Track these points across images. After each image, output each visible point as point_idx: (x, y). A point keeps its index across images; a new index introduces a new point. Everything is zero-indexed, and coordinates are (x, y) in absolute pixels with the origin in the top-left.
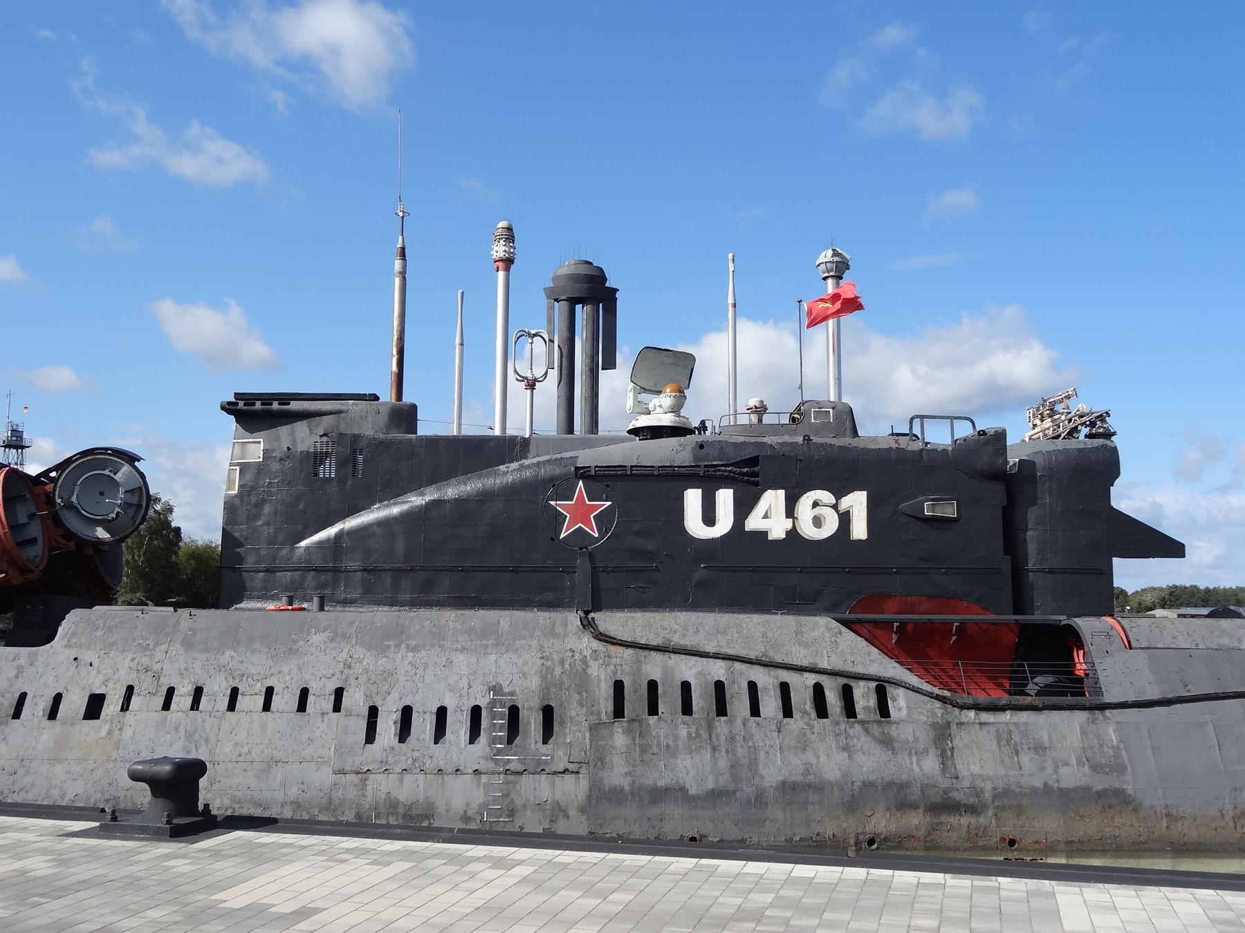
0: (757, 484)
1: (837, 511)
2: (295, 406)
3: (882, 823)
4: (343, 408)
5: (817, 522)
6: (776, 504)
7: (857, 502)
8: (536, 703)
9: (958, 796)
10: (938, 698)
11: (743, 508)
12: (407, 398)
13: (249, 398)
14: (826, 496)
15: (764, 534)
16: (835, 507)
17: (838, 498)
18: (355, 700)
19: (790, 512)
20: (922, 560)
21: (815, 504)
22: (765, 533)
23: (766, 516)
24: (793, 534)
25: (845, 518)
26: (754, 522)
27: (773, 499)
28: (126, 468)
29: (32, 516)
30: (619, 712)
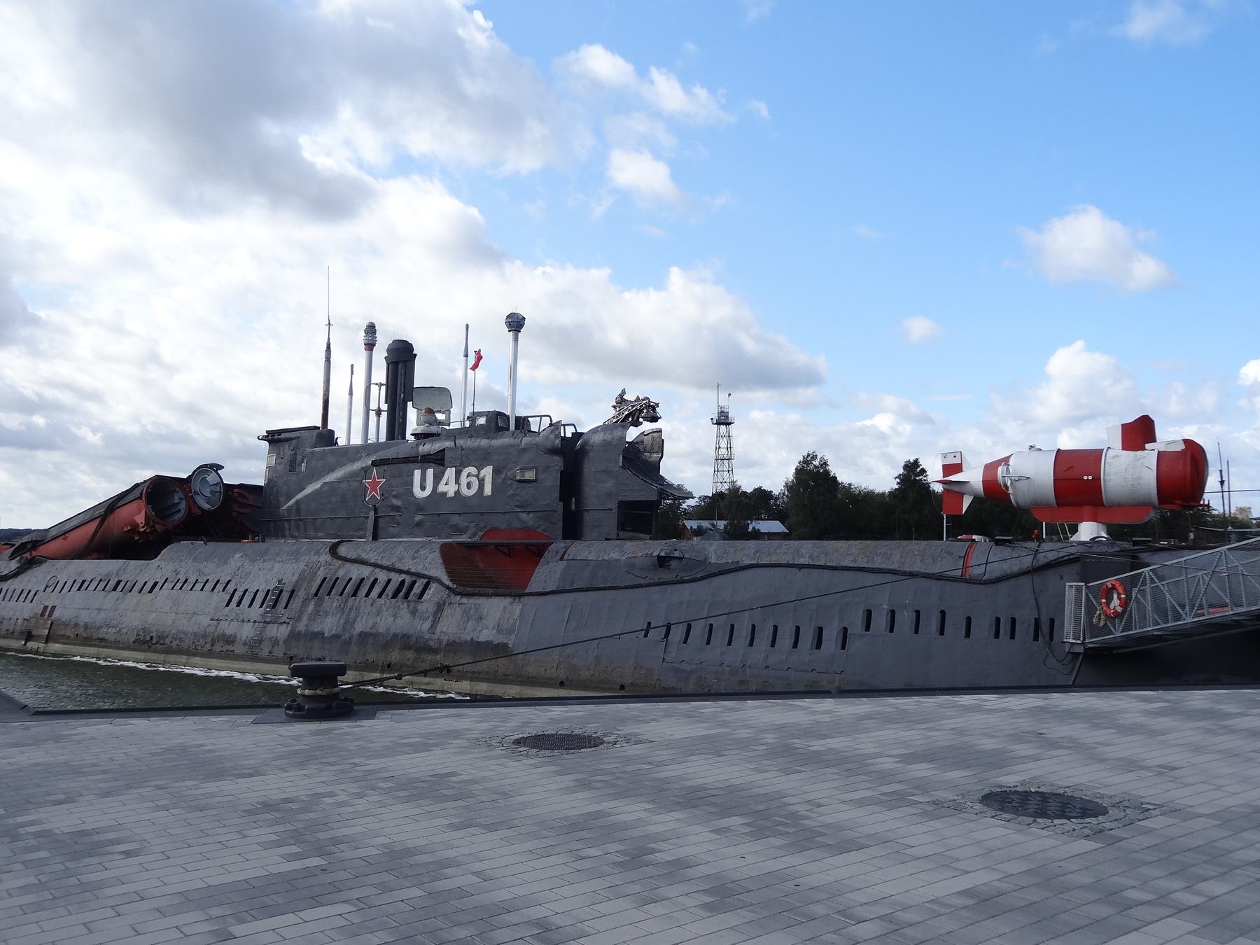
2: (283, 436)
3: (395, 656)
5: (469, 486)
7: (487, 472)
8: (290, 589)
9: (431, 643)
10: (448, 588)
11: (438, 478)
12: (329, 427)
14: (472, 470)
15: (445, 494)
16: (477, 476)
18: (231, 588)
19: (457, 481)
21: (469, 475)
24: (457, 493)
25: (481, 482)
26: (442, 488)
27: (450, 473)
30: (316, 595)
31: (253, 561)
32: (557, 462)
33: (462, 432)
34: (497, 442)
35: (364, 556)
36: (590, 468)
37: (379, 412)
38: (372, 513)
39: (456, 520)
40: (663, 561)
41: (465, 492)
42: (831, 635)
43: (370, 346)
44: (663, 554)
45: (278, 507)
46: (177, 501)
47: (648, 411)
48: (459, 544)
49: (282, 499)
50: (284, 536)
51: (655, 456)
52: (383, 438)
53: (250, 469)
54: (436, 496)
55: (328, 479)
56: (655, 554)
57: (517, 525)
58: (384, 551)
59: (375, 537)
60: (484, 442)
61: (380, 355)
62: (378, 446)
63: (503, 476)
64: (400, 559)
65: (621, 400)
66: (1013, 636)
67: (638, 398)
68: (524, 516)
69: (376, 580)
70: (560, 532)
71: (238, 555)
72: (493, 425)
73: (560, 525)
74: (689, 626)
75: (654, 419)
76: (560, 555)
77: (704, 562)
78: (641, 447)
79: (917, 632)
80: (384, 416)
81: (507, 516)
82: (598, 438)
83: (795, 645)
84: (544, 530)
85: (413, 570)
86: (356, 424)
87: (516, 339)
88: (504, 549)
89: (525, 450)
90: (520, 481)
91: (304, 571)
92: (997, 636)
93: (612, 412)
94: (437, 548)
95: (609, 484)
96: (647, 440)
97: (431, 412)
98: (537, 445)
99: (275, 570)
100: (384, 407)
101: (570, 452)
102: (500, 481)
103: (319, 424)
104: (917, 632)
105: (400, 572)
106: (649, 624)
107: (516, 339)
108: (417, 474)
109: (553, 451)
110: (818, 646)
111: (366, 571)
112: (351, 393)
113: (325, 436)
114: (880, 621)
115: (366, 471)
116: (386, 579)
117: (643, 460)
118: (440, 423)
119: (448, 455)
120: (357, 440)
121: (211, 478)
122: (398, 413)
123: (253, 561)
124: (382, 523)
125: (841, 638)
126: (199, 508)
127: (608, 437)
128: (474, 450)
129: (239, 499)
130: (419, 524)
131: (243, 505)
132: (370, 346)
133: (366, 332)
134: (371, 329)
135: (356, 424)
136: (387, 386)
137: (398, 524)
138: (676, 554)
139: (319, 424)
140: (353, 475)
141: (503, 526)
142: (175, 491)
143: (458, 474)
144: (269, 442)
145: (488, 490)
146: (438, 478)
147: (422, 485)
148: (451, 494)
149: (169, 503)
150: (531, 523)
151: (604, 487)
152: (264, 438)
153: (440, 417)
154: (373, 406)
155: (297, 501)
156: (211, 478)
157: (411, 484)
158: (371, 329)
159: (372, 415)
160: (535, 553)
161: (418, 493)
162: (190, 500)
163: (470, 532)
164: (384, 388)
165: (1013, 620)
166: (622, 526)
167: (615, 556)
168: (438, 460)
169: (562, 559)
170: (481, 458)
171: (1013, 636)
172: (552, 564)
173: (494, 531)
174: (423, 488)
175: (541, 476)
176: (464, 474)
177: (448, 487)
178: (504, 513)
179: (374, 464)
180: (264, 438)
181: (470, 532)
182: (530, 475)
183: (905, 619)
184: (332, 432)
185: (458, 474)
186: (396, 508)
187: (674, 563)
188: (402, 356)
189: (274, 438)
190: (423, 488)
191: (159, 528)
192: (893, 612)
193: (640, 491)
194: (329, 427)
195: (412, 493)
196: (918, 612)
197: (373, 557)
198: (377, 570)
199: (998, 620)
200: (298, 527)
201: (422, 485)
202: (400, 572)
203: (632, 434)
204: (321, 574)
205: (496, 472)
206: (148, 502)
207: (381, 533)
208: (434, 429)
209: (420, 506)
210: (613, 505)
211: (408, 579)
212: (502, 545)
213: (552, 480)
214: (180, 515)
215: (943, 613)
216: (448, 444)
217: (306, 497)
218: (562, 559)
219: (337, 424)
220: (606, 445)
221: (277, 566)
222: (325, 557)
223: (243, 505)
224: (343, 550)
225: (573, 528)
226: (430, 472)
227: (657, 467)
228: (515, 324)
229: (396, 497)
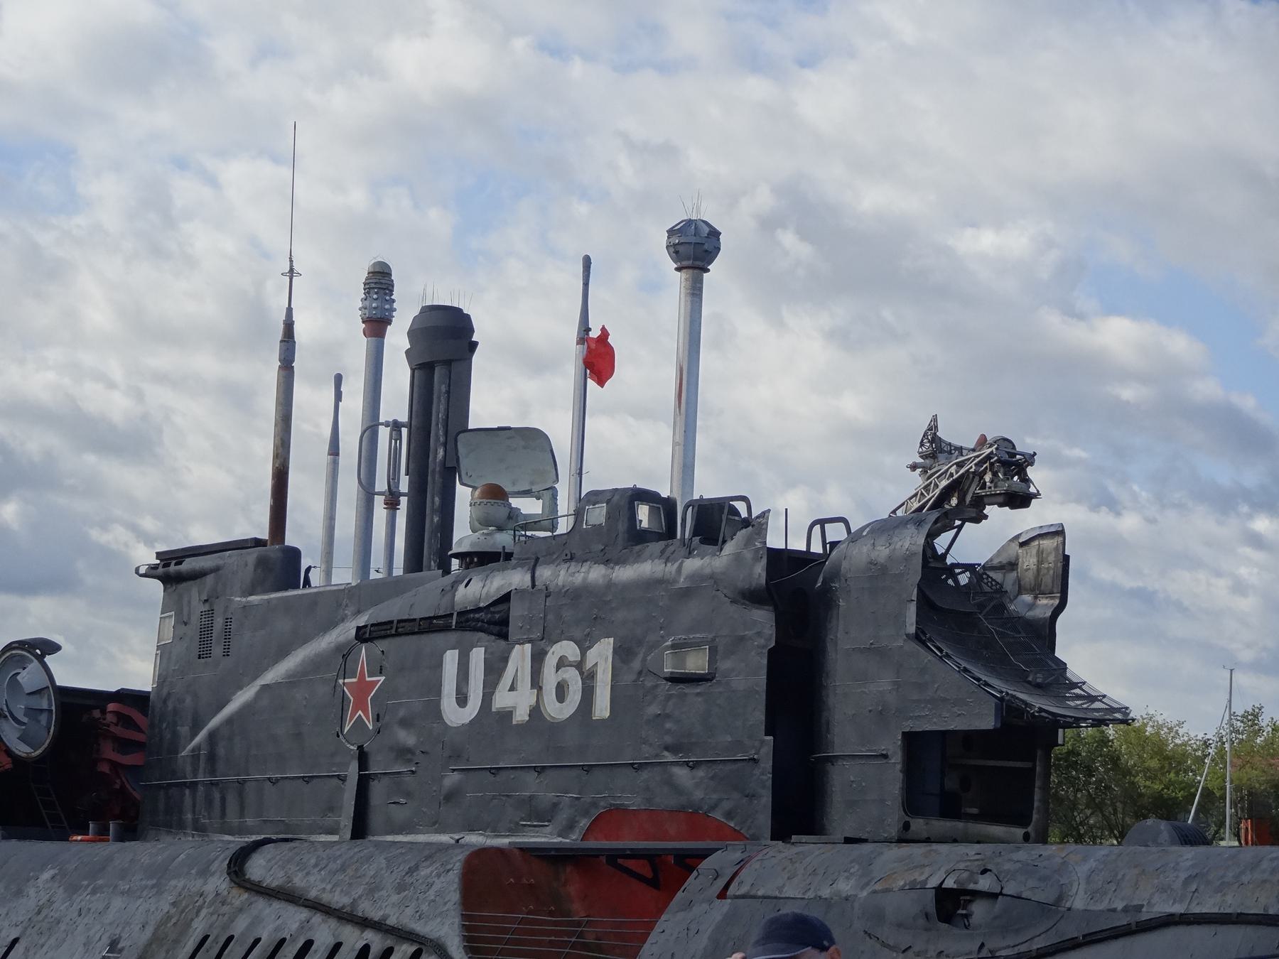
0: (504, 636)
1: (581, 673)
2: (189, 565)
4: (221, 562)
6: (523, 667)
7: (602, 653)
12: (291, 540)
13: (166, 558)
15: (507, 715)
16: (579, 666)
17: (583, 654)
19: (536, 683)
20: (667, 748)
21: (562, 663)
23: (512, 688)
24: (536, 711)
25: (589, 679)
26: (502, 699)
27: (520, 656)
28: (34, 665)
31: (73, 889)
32: (763, 621)
33: (569, 549)
34: (625, 573)
35: (299, 881)
36: (847, 638)
37: (392, 504)
38: (353, 770)
39: (532, 786)
40: (950, 905)
41: (558, 711)
43: (377, 325)
44: (949, 884)
45: (174, 749)
47: (1001, 475)
48: (525, 850)
49: (184, 730)
50: (181, 826)
51: (1045, 605)
52: (398, 570)
53: (116, 650)
54: (493, 722)
55: (270, 677)
56: (933, 883)
57: (665, 800)
58: (343, 869)
59: (360, 830)
60: (595, 574)
61: (397, 339)
62: (390, 587)
63: (636, 665)
64: (373, 890)
65: (935, 447)
67: (983, 441)
68: (681, 774)
69: (309, 944)
70: (764, 820)
71: (46, 875)
72: (622, 526)
73: (766, 799)
75: (1019, 500)
76: (720, 884)
77: (1052, 909)
78: (1009, 581)
80: (404, 501)
81: (645, 775)
82: (862, 553)
84: (729, 815)
85: (392, 921)
86: (344, 534)
87: (695, 291)
88: (644, 869)
89: (686, 594)
90: (675, 679)
91: (168, 917)
93: (916, 481)
94: (457, 862)
95: (883, 684)
96: (1028, 561)
97: (496, 493)
98: (714, 579)
99: (110, 917)
100: (404, 485)
101: (797, 591)
102: (628, 678)
103: (262, 531)
105: (365, 923)
108: (451, 659)
109: (753, 597)
111: (291, 920)
112: (334, 450)
113: (277, 563)
115: (345, 654)
116: (331, 941)
117: (996, 622)
118: (534, 523)
119: (517, 611)
120: (344, 576)
121: (29, 677)
122: (433, 500)
123: (73, 889)
124: (378, 791)
126: (8, 752)
127: (882, 552)
128: (575, 595)
129: (118, 731)
130: (451, 797)
131: (125, 745)
132: (377, 325)
133: (368, 288)
134: (380, 281)
135: (344, 534)
136: (409, 425)
137: (408, 795)
138: (984, 884)
139: (264, 534)
140: (316, 665)
141: (633, 802)
143: (538, 659)
144: (167, 580)
145: (602, 708)
146: (494, 670)
147: (465, 690)
148: (521, 715)
150: (698, 794)
151: (883, 690)
152: (152, 572)
153: (529, 507)
154: (381, 484)
155: (212, 736)
156: (29, 677)
157: (437, 689)
158: (380, 281)
159: (379, 502)
160: (665, 873)
161: (456, 716)
163: (562, 817)
164: (405, 431)
166: (913, 803)
167: (845, 887)
168: (493, 622)
169: (722, 895)
170: (585, 614)
172: (697, 909)
173: (611, 818)
174: (462, 700)
175: (724, 665)
176: (551, 660)
177: (516, 700)
178: (638, 767)
179: (363, 635)
180: (152, 572)
181: (562, 817)
182: (696, 663)
184: (294, 554)
185: (538, 659)
186: (403, 753)
187: (979, 910)
188: (446, 344)
189: (174, 570)
190: (462, 700)
193: (964, 701)
195: (435, 711)
197: (314, 885)
198: (318, 918)
200: (209, 802)
201: (465, 690)
202: (365, 923)
203: (978, 542)
204: (198, 927)
205: (623, 654)
207: (376, 819)
208: (503, 540)
209: (455, 748)
210: (892, 745)
212: (635, 855)
213: (749, 675)
216: (516, 579)
217: (229, 721)
218: (722, 895)
219: (303, 532)
220: (878, 573)
221: (118, 903)
222: (219, 882)
223: (125, 745)
224: (257, 868)
225: (799, 807)
226: (478, 656)
227: (1045, 633)
228: (695, 249)
229: (405, 723)
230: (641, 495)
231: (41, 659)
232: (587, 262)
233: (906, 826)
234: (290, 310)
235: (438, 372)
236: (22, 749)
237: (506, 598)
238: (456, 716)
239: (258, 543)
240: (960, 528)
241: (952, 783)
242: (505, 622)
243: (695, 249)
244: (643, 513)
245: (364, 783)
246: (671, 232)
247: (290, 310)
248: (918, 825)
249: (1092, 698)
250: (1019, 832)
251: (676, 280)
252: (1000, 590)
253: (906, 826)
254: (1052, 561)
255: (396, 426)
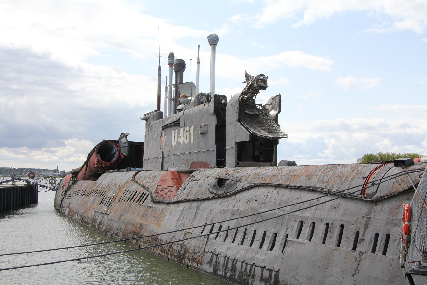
13: (145, 115)
16: (189, 132)
21: (187, 132)
22: (180, 142)
24: (184, 142)
25: (190, 134)
29: (116, 151)
42: (280, 239)
43: (171, 65)
46: (114, 152)
53: (138, 134)
66: (384, 253)
74: (213, 225)
79: (324, 242)
83: (261, 247)
87: (214, 50)
92: (374, 251)
104: (324, 242)
106: (206, 224)
107: (214, 50)
110: (271, 249)
113: (159, 115)
114: (306, 230)
121: (123, 140)
125: (283, 243)
134: (172, 56)
142: (113, 148)
148: (182, 143)
149: (112, 153)
156: (123, 140)
158: (172, 56)
161: (174, 144)
162: (119, 151)
165: (388, 236)
171: (384, 253)
177: (181, 140)
183: (320, 229)
184: (162, 113)
188: (179, 67)
191: (104, 165)
192: (314, 223)
194: (161, 111)
196: (327, 224)
199: (377, 235)
202: (145, 188)
206: (98, 153)
210: (234, 145)
211: (145, 191)
214: (115, 159)
215: (342, 226)
219: (162, 110)
228: (213, 41)
230: (202, 94)
231: (126, 136)
232: (199, 46)
233: (238, 163)
234: (160, 64)
235: (178, 73)
236: (125, 154)
237: (179, 119)
238: (174, 144)
239: (156, 111)
240: (256, 96)
241: (257, 153)
242: (179, 124)
243: (213, 41)
244: (204, 99)
245: (163, 158)
246: (208, 37)
247: (160, 64)
248: (241, 163)
249: (282, 132)
250: (270, 164)
251: (210, 47)
252: (267, 110)
253: (238, 163)
254: (278, 103)
255: (173, 85)
